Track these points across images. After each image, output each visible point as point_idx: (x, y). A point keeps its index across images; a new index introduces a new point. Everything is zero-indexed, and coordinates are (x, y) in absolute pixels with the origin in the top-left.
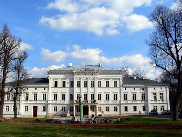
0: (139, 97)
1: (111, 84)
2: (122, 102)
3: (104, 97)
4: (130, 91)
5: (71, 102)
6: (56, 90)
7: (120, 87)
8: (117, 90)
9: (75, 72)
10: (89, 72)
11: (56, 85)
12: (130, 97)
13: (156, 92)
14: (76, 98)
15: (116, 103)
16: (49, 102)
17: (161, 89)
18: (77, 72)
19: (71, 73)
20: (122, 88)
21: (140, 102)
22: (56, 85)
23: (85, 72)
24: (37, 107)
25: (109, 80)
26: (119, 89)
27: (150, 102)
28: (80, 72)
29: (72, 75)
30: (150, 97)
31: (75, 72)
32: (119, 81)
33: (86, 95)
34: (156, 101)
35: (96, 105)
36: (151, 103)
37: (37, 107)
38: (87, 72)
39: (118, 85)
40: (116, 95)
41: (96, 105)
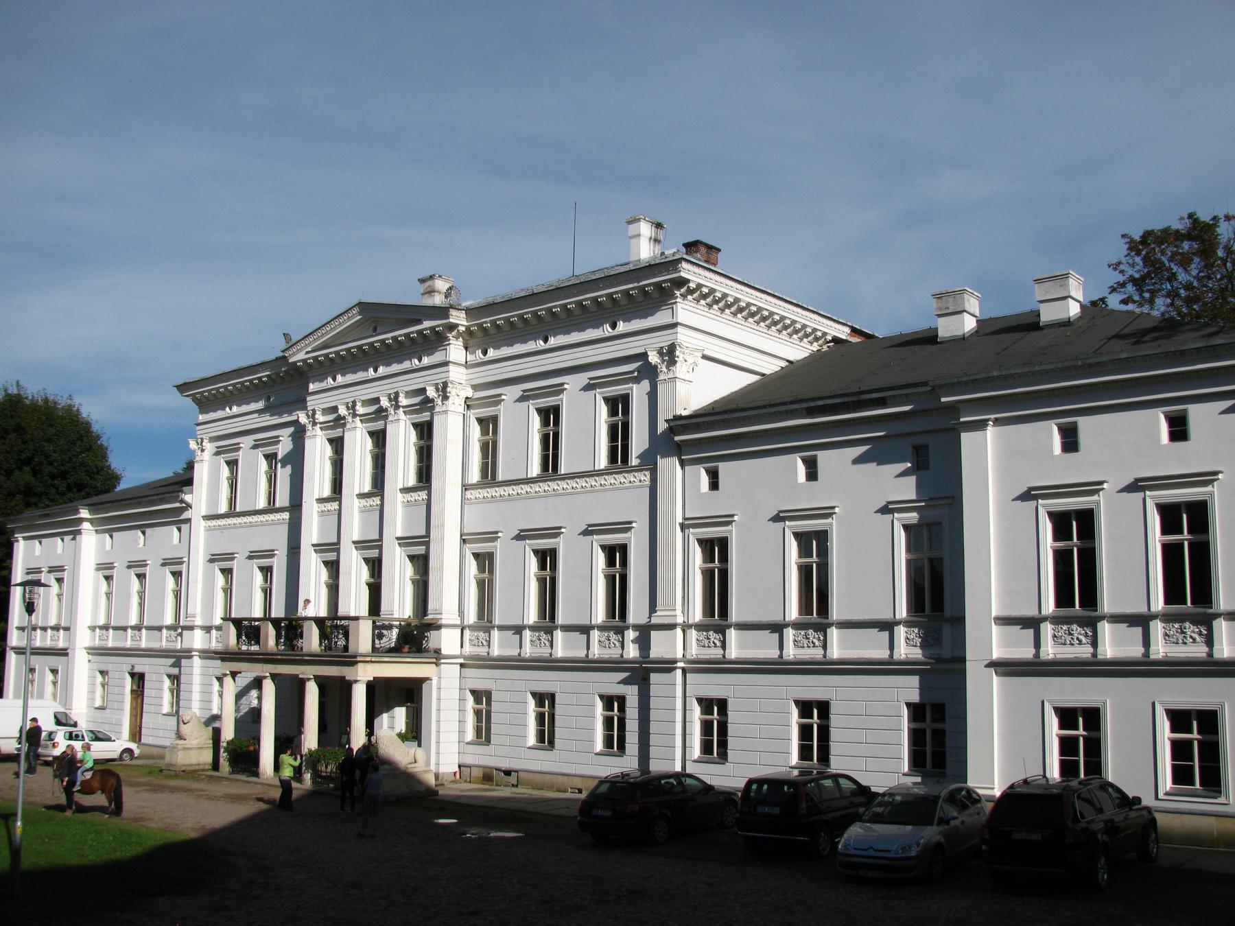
0: (870, 573)
1: (587, 428)
2: (660, 646)
7: (649, 461)
8: (622, 498)
12: (767, 580)
13: (1093, 488)
15: (614, 653)
17: (1179, 429)
20: (669, 467)
21: (872, 647)
25: (558, 390)
26: (645, 477)
27: (988, 641)
30: (1004, 566)
31: (301, 356)
32: (645, 385)
34: (1091, 623)
35: (347, 672)
36: (997, 654)
39: (639, 442)
41: (347, 672)
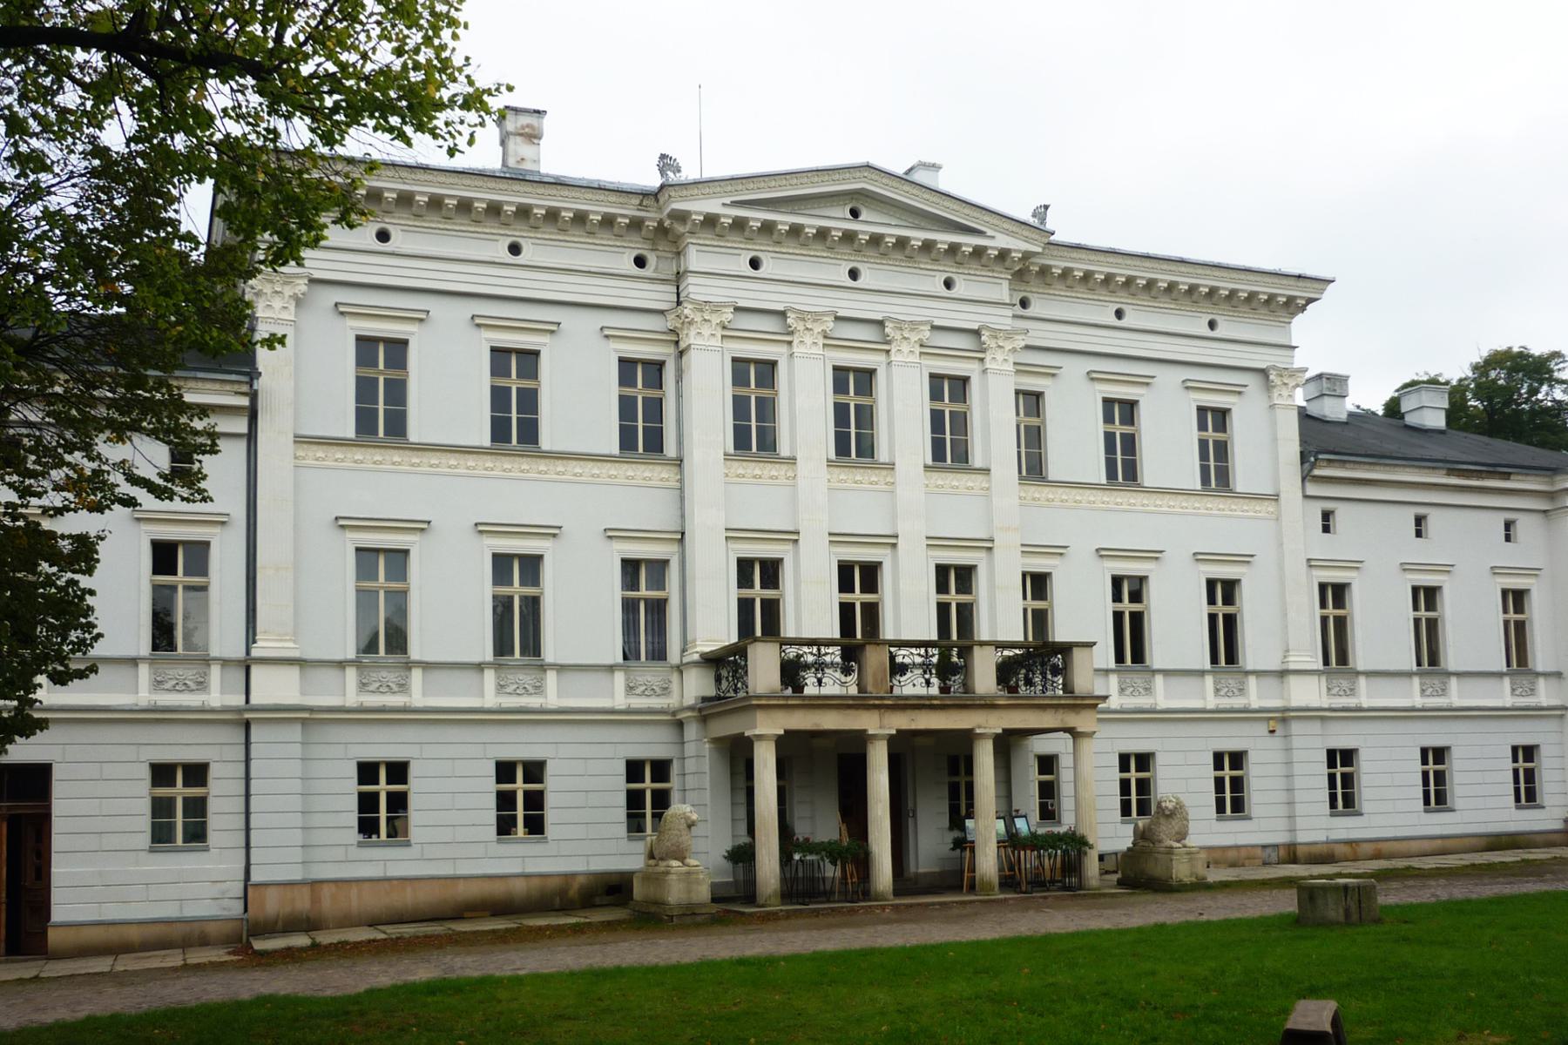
3: (1177, 629)
4: (1379, 544)
5: (630, 689)
6: (380, 486)
9: (711, 221)
10: (902, 243)
11: (381, 411)
14: (710, 619)
16: (272, 688)
18: (739, 225)
19: (636, 225)
22: (381, 411)
23: (849, 237)
24: (50, 766)
28: (784, 220)
29: (640, 262)
31: (713, 206)
33: (859, 577)
37: (50, 766)
38: (876, 240)
40: (1223, 591)
